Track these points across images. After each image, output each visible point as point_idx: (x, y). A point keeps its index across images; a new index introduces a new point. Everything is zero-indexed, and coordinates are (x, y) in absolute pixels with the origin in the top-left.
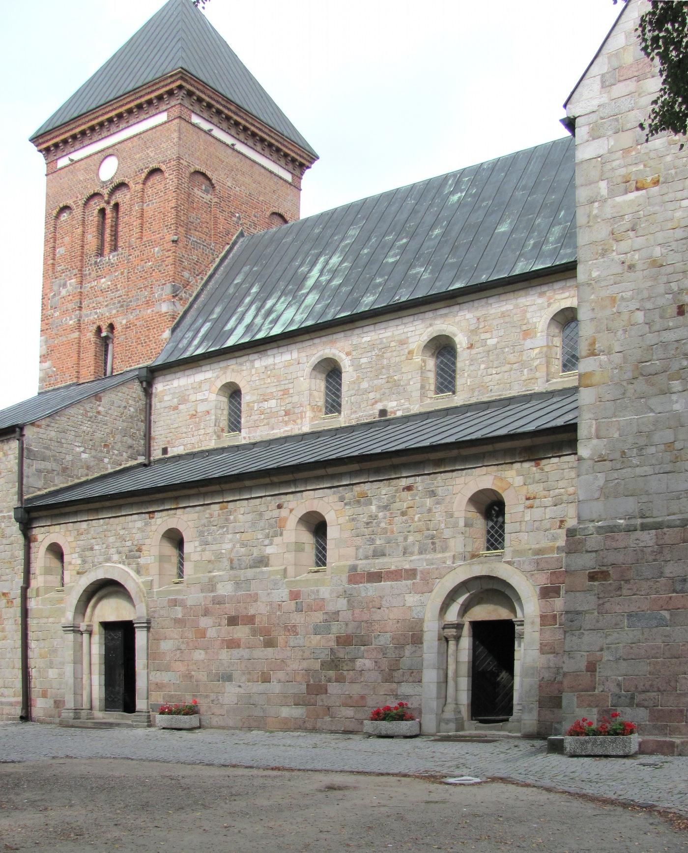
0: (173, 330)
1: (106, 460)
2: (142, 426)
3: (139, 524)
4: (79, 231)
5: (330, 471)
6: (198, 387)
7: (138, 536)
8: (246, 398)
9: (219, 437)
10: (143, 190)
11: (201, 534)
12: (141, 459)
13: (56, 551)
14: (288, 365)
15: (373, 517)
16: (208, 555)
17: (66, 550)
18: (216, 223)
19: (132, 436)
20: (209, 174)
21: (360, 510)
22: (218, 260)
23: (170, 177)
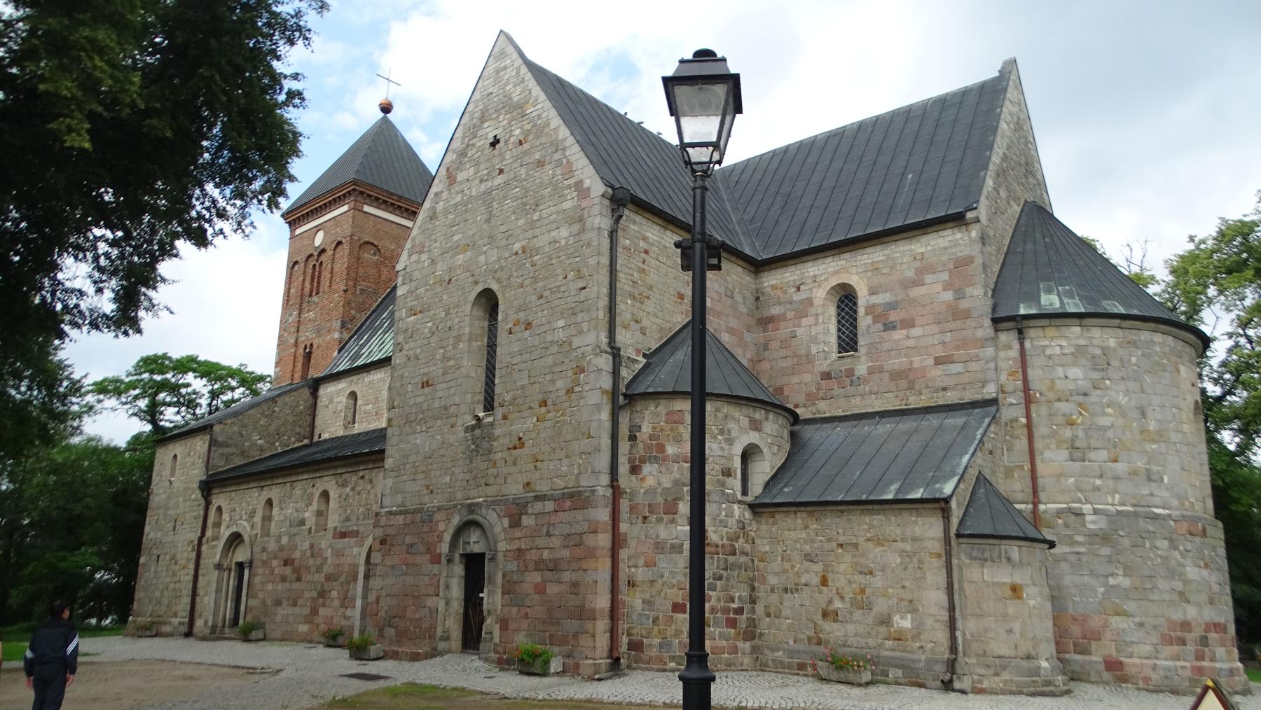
0: (339, 352)
1: (277, 444)
2: (309, 419)
3: (256, 494)
4: (301, 278)
5: (332, 464)
6: (338, 393)
7: (255, 502)
8: (359, 402)
9: (346, 428)
10: (334, 255)
11: (280, 501)
12: (306, 441)
13: (219, 509)
14: (380, 380)
15: (348, 495)
16: (282, 517)
17: (224, 511)
18: (380, 275)
19: (300, 426)
20: (375, 242)
21: (343, 490)
22: (380, 300)
23: (345, 247)
